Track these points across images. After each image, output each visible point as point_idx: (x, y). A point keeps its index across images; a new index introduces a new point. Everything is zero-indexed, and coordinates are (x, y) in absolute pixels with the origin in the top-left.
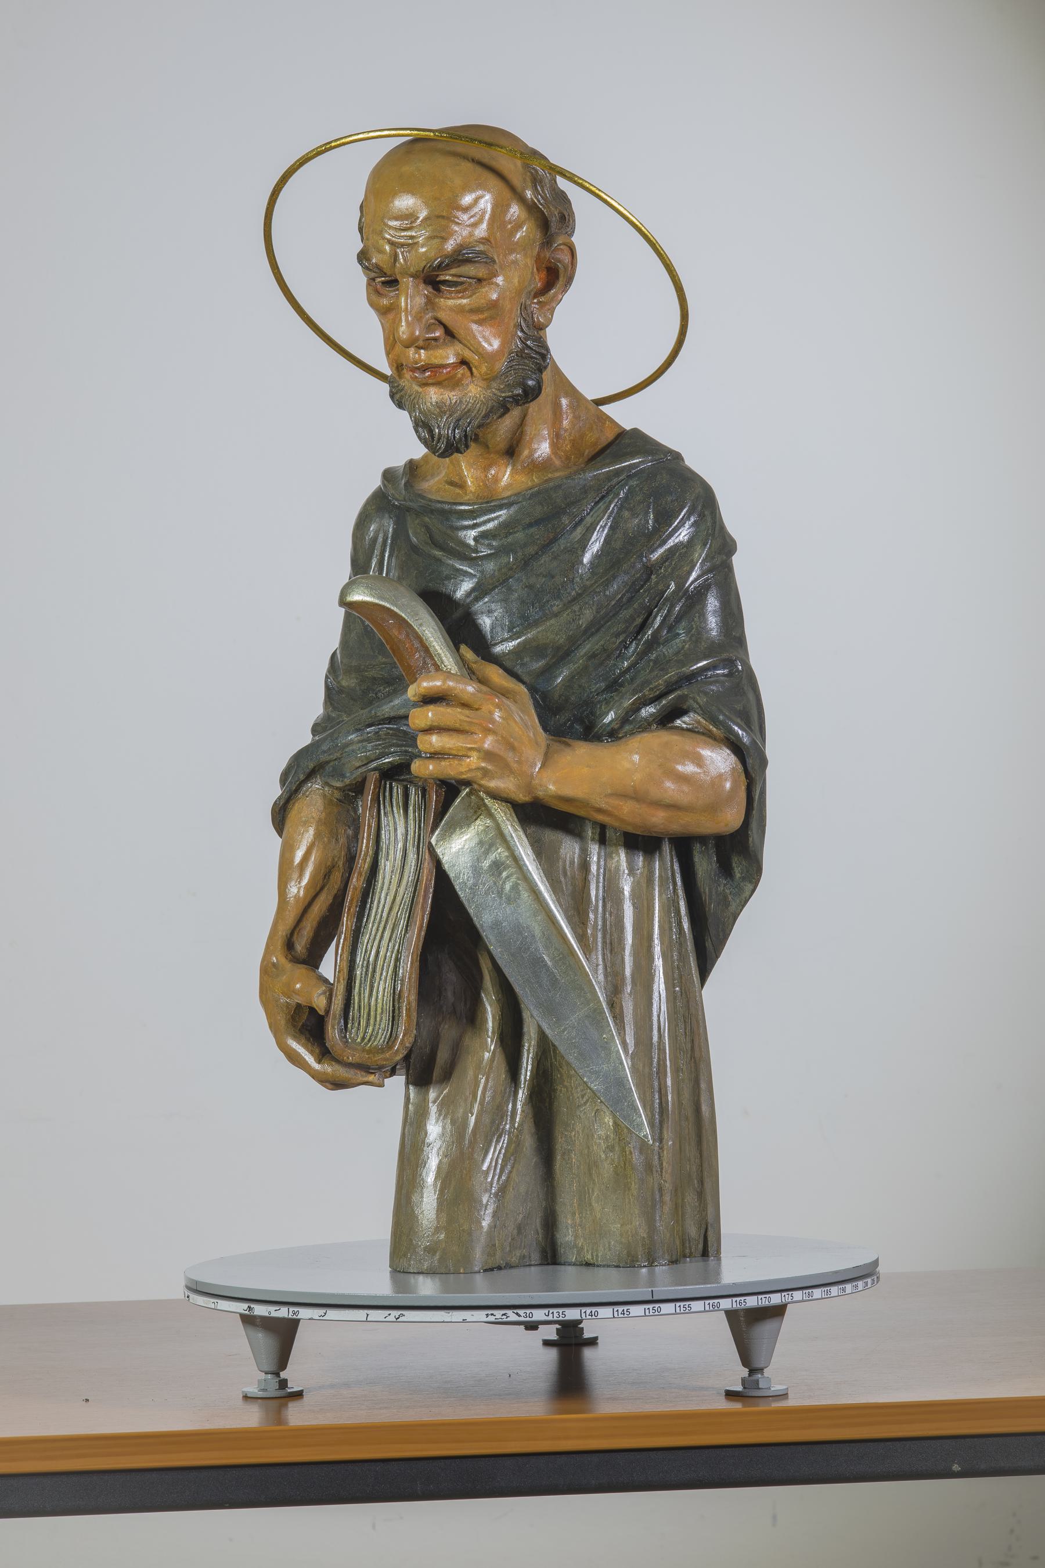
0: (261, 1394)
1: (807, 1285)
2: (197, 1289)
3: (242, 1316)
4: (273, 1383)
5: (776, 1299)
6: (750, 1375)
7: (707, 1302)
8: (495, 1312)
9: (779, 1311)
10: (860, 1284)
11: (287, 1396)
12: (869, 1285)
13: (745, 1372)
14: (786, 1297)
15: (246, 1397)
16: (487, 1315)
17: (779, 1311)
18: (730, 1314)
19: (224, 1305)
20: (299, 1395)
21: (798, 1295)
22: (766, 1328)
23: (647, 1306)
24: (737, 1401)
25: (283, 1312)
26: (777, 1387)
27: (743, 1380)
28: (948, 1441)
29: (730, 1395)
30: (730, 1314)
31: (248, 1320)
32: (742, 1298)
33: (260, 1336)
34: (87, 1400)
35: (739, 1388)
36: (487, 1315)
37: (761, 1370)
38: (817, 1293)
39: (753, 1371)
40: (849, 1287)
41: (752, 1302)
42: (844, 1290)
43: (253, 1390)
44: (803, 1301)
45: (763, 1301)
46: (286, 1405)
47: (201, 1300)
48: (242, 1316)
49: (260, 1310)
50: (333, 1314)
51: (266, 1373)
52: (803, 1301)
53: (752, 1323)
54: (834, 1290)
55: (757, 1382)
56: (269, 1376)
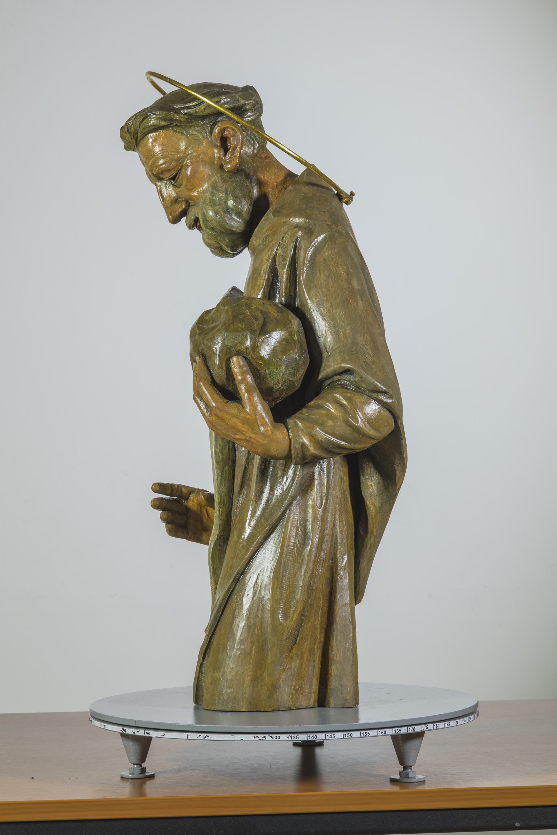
0: (130, 776)
1: (436, 721)
2: (96, 717)
3: (121, 734)
4: (137, 769)
5: (418, 729)
6: (404, 770)
7: (379, 731)
8: (259, 736)
9: (420, 735)
10: (467, 719)
11: (144, 778)
12: (472, 719)
13: (401, 768)
14: (424, 728)
15: (122, 778)
16: (255, 737)
17: (420, 735)
18: (394, 737)
19: (109, 727)
20: (152, 777)
21: (430, 726)
22: (413, 744)
23: (344, 733)
24: (396, 785)
25: (141, 733)
26: (420, 777)
27: (400, 773)
28: (513, 810)
29: (393, 781)
30: (394, 737)
31: (124, 736)
32: (399, 729)
33: (130, 744)
34: (33, 778)
35: (397, 777)
36: (255, 737)
37: (410, 767)
38: (442, 725)
39: (405, 768)
40: (460, 721)
41: (404, 730)
42: (457, 723)
43: (126, 774)
44: (433, 729)
45: (410, 730)
46: (145, 783)
47: (97, 724)
48: (121, 734)
49: (129, 731)
50: (169, 735)
51: (134, 764)
52: (433, 729)
53: (405, 741)
54: (452, 723)
55: (408, 774)
56: (136, 766)
